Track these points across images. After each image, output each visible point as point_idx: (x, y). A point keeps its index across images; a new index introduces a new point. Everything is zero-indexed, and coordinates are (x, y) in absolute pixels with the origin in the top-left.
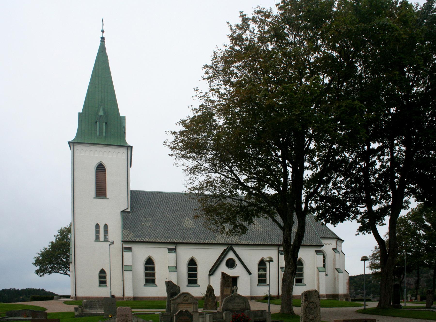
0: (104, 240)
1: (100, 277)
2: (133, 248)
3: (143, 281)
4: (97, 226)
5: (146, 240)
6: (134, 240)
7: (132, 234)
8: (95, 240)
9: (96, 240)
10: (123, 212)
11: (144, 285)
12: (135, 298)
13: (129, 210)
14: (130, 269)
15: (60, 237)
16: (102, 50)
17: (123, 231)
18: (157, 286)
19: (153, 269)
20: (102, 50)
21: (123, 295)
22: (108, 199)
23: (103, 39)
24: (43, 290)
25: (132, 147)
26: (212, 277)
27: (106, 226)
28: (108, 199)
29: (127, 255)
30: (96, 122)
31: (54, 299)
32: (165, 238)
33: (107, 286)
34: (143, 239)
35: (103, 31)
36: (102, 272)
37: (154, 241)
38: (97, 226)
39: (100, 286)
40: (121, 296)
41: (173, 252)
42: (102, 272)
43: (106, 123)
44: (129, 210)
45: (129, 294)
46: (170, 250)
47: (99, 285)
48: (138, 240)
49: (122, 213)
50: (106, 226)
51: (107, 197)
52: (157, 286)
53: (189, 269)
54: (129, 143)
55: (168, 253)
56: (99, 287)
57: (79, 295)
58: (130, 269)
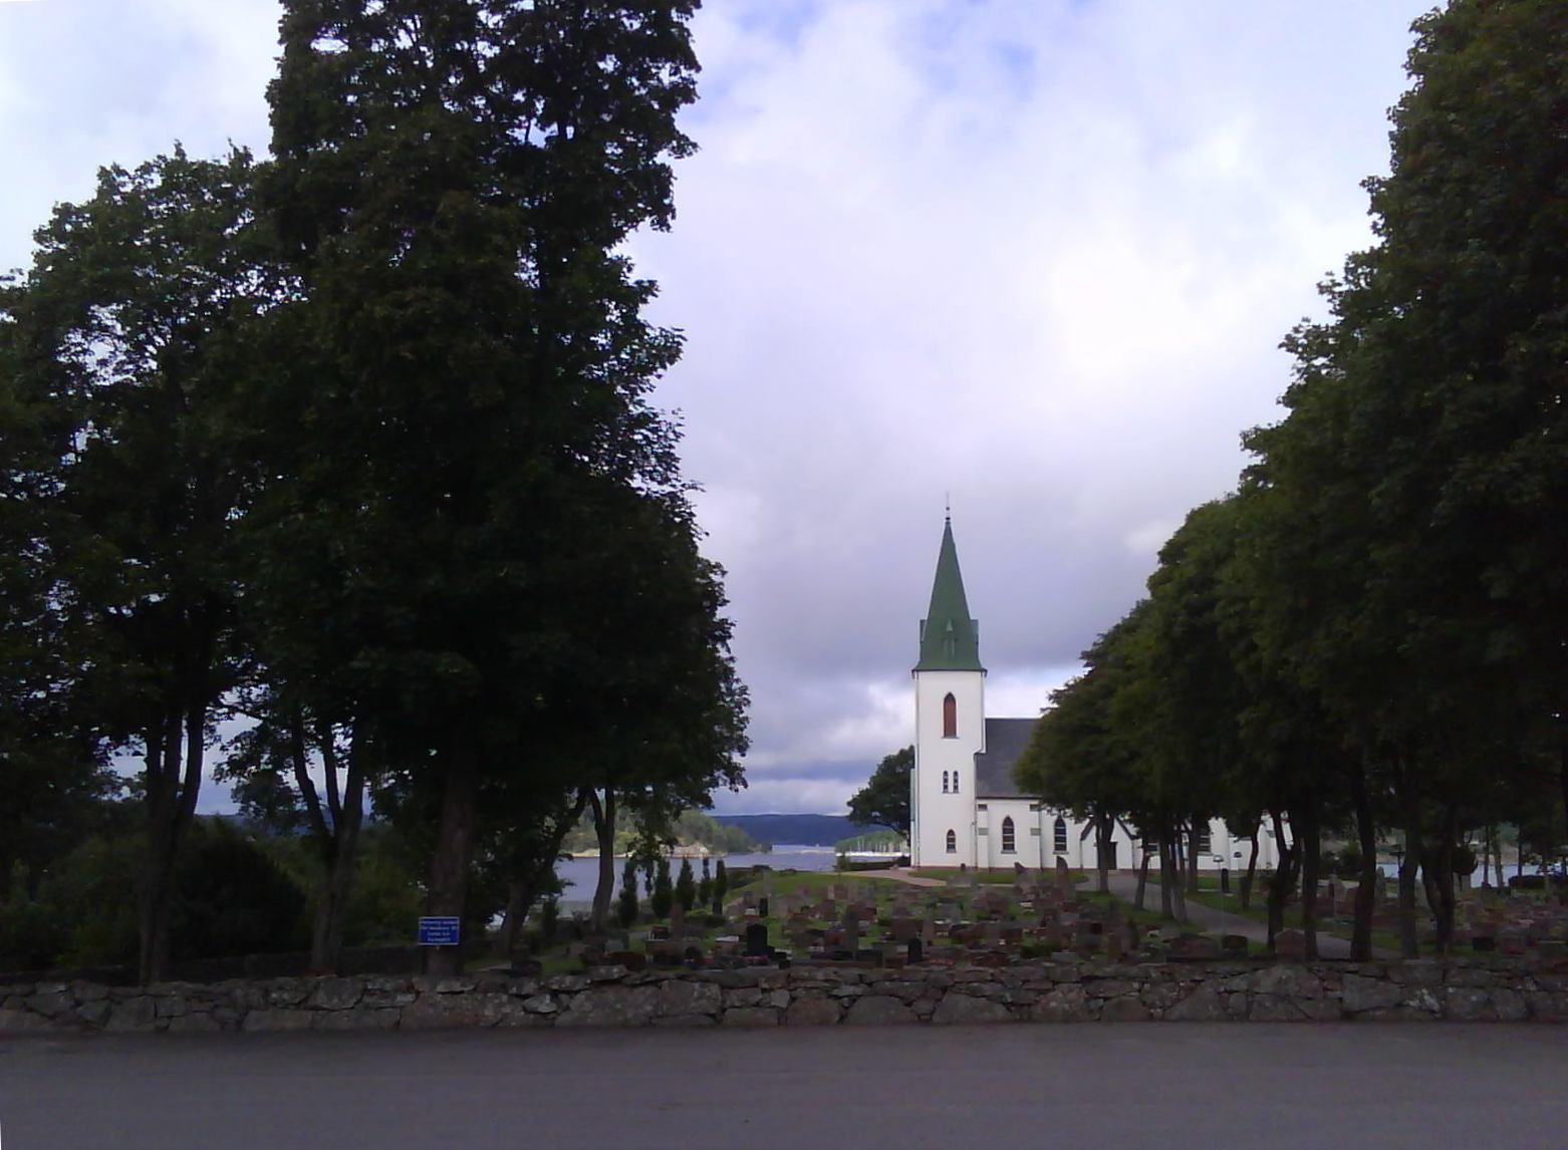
1: (948, 840)
2: (988, 807)
3: (1000, 847)
4: (946, 773)
10: (976, 754)
11: (1002, 853)
12: (990, 869)
13: (984, 751)
14: (984, 832)
16: (948, 533)
18: (1015, 853)
19: (1012, 831)
20: (948, 533)
23: (948, 518)
26: (1083, 842)
27: (956, 773)
29: (982, 814)
35: (948, 509)
36: (951, 832)
38: (946, 773)
40: (974, 865)
42: (951, 832)
43: (956, 640)
44: (984, 751)
45: (983, 864)
46: (1032, 807)
50: (956, 773)
52: (1015, 853)
53: (1057, 832)
54: (984, 666)
57: (921, 865)
58: (984, 832)
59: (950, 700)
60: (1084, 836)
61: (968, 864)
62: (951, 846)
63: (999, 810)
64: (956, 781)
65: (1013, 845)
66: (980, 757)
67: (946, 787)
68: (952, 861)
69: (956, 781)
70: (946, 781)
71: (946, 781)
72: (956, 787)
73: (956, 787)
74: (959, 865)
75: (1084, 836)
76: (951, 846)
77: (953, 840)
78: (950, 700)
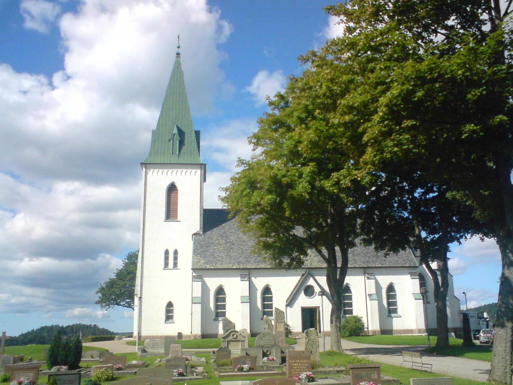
0: (173, 268)
4: (167, 252)
5: (218, 266)
6: (204, 268)
7: (203, 261)
8: (163, 268)
9: (165, 268)
10: (195, 234)
15: (127, 261)
17: (193, 257)
19: (224, 300)
21: (191, 333)
22: (180, 221)
24: (103, 328)
25: (205, 165)
27: (176, 252)
28: (180, 221)
30: (170, 141)
31: (115, 339)
32: (239, 263)
33: (173, 321)
34: (214, 265)
36: (170, 305)
37: (226, 267)
38: (167, 252)
39: (166, 322)
41: (246, 279)
42: (170, 305)
47: (166, 321)
48: (208, 267)
49: (194, 236)
50: (176, 252)
51: (179, 219)
55: (241, 280)
56: (166, 323)
59: (172, 189)
60: (290, 302)
61: (186, 332)
62: (169, 317)
63: (213, 283)
64: (176, 258)
65: (225, 312)
66: (198, 237)
67: (166, 265)
68: (171, 330)
69: (176, 258)
70: (167, 259)
71: (167, 259)
72: (175, 265)
73: (175, 265)
74: (177, 334)
75: (290, 302)
76: (169, 317)
77: (172, 311)
78: (172, 189)
